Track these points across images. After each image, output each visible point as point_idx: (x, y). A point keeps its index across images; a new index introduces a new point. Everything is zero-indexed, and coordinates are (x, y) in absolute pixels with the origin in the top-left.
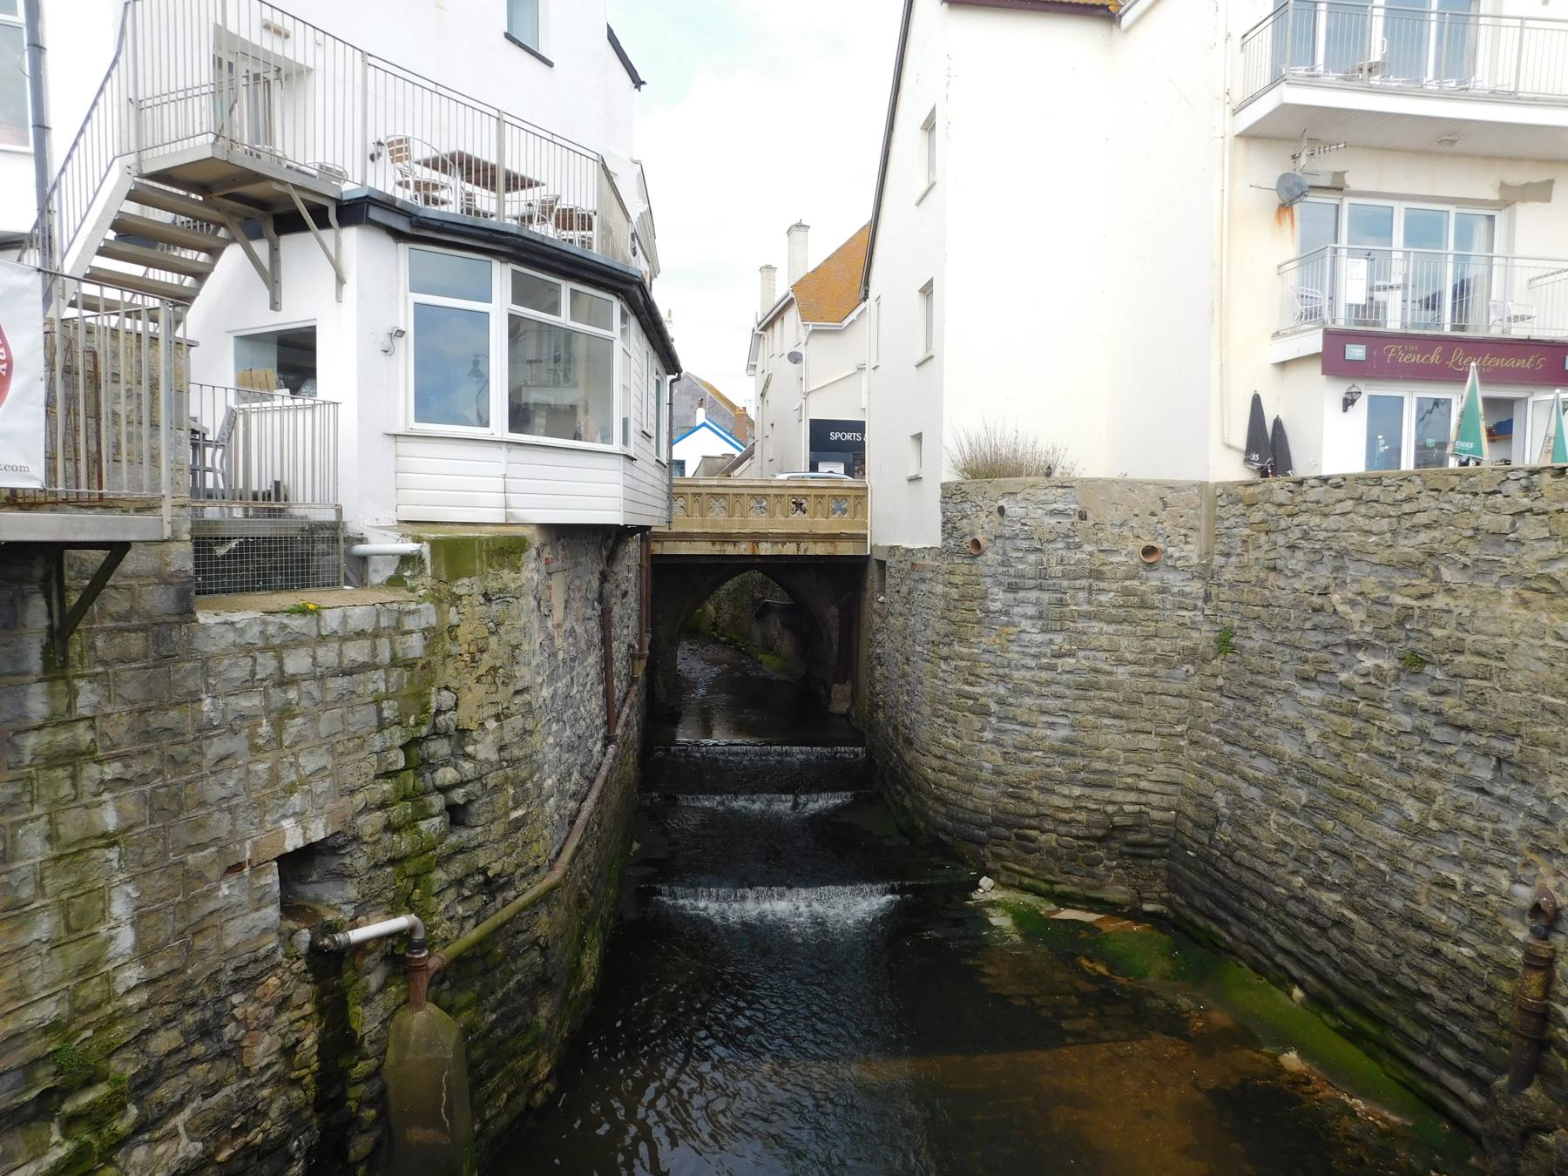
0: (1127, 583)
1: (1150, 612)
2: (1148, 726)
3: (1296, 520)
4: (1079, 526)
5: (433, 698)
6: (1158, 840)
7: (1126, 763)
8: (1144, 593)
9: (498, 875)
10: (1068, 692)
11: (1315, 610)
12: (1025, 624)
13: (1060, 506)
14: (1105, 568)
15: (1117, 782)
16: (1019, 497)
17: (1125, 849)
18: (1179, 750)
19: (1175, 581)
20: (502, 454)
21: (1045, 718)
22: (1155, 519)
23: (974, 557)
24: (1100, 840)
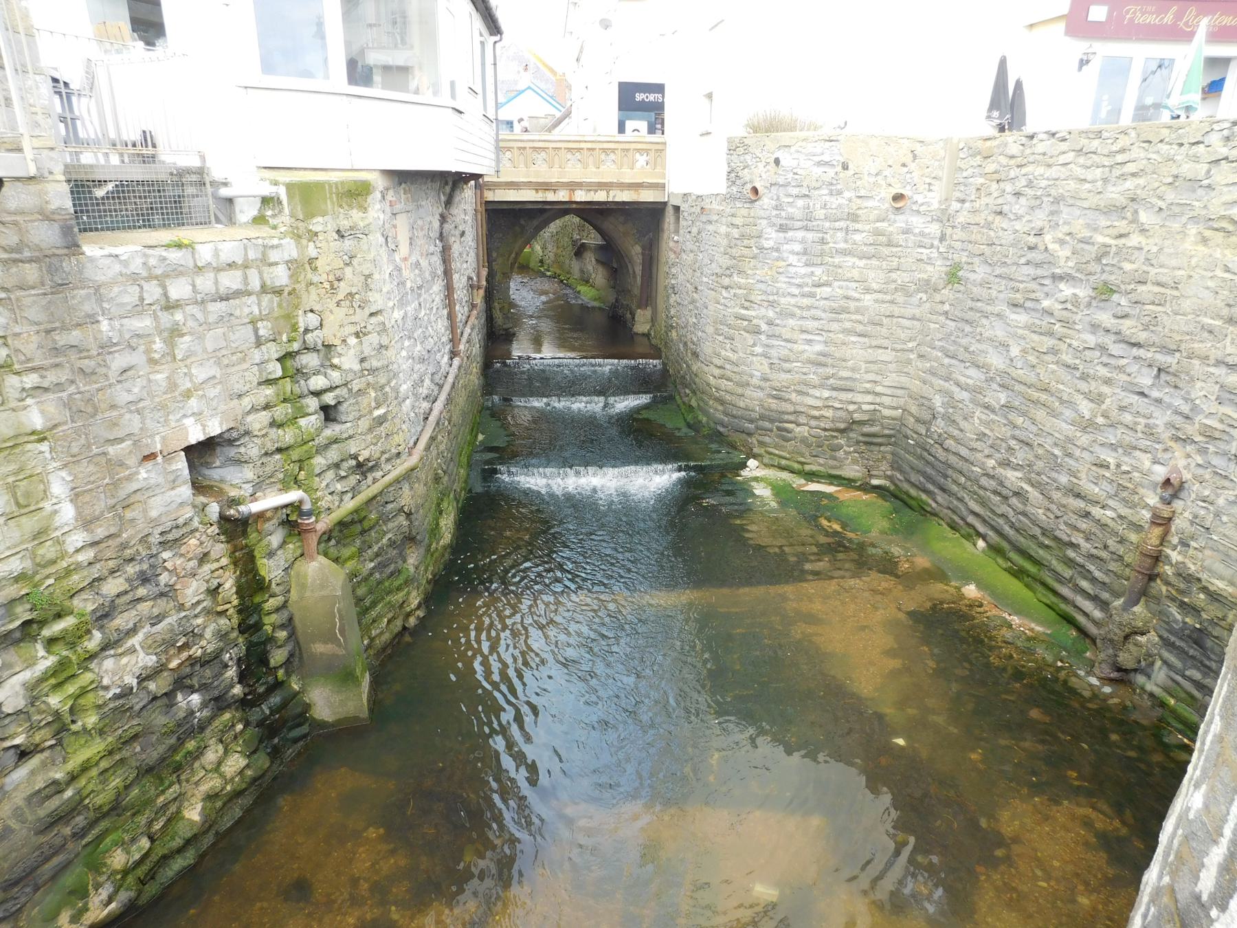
0: (878, 224)
1: (894, 249)
2: (885, 343)
3: (1024, 170)
4: (841, 175)
5: (301, 319)
6: (887, 432)
7: (866, 372)
8: (891, 233)
9: (368, 460)
10: (823, 315)
11: (1030, 248)
12: (793, 259)
13: (826, 158)
14: (860, 212)
15: (859, 387)
16: (793, 149)
17: (861, 438)
18: (909, 362)
19: (917, 222)
21: (805, 336)
22: (905, 169)
23: (753, 202)
24: (842, 431)
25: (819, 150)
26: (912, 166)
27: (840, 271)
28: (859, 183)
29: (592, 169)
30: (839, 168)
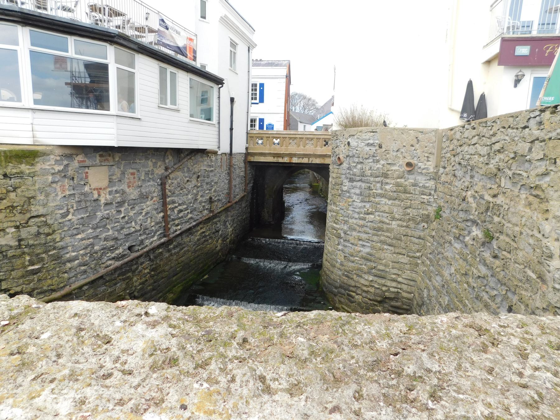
0: (398, 180)
1: (408, 195)
2: (404, 251)
4: (379, 151)
6: (405, 307)
7: (393, 268)
8: (406, 186)
10: (370, 231)
12: (355, 197)
13: (371, 142)
14: (389, 172)
15: (389, 276)
16: (355, 137)
17: (390, 308)
18: (417, 265)
19: (422, 180)
20: (29, 114)
21: (361, 242)
22: (413, 148)
24: (380, 302)
25: (368, 137)
26: (417, 146)
27: (378, 206)
28: (388, 156)
29: (302, 147)
30: (377, 148)
